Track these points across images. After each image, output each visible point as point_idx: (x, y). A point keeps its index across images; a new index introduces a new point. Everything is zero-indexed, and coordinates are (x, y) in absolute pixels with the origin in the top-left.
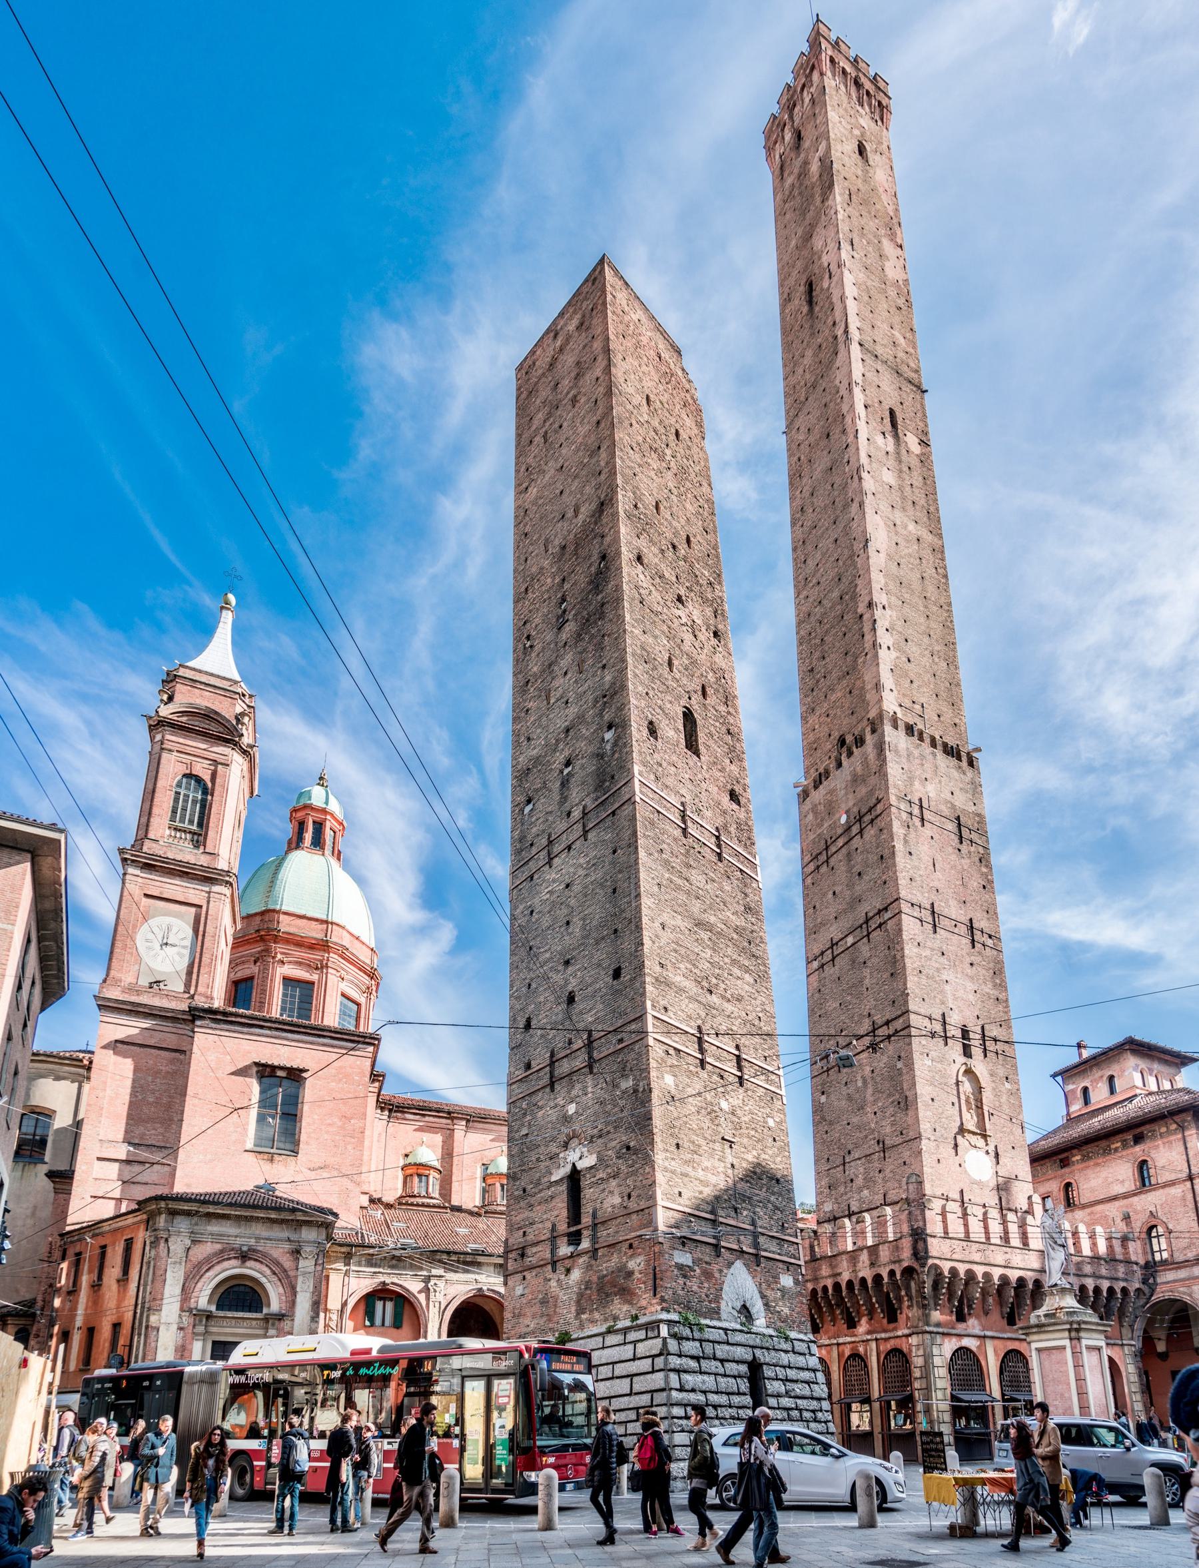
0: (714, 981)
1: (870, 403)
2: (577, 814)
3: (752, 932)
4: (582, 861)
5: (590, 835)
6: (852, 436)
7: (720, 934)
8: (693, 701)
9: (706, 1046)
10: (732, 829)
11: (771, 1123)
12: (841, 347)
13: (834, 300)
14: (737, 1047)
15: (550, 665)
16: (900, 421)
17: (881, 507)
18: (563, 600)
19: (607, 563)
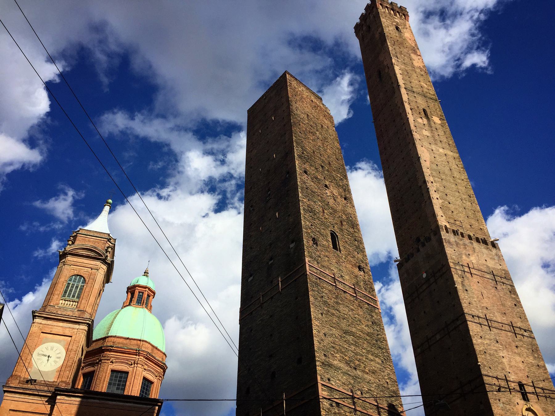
0: (357, 362)
1: (412, 108)
7: (359, 337)
9: (356, 400)
10: (362, 284)
16: (429, 113)
17: (424, 144)
18: (269, 190)
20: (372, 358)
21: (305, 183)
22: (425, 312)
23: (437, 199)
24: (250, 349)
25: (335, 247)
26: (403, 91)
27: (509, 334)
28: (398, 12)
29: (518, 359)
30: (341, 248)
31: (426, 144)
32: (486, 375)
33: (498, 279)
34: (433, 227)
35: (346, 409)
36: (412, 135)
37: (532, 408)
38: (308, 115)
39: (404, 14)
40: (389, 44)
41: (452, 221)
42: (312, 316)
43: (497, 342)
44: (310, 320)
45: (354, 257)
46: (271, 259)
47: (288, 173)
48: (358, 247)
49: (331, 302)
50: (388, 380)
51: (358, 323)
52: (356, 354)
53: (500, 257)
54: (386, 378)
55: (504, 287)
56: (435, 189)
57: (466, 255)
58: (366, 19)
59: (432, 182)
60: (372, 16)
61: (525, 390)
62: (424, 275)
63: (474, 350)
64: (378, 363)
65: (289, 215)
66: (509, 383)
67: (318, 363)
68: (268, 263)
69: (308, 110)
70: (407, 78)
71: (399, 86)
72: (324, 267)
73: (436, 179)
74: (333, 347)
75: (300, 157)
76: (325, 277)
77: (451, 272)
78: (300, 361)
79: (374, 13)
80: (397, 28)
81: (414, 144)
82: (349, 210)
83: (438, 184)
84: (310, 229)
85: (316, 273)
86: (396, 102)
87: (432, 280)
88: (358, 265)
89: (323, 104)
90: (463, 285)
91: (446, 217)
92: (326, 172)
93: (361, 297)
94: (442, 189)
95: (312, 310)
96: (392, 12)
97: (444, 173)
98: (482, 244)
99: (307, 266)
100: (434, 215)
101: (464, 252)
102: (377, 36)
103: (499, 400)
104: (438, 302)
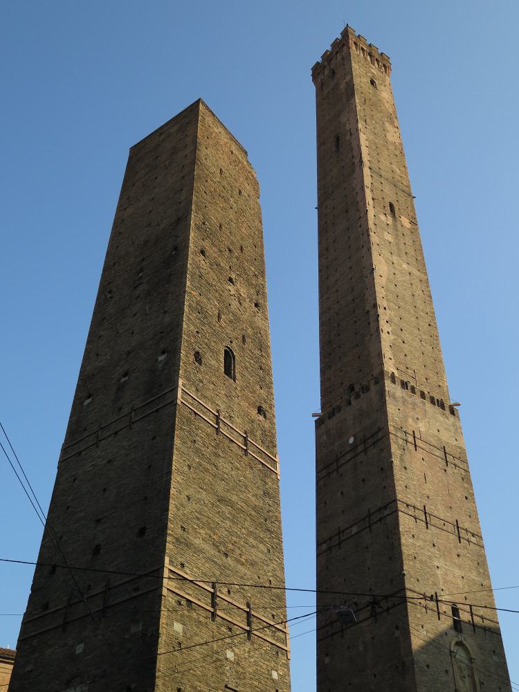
2: (126, 410)
3: (269, 511)
6: (363, 213)
7: (241, 511)
8: (234, 344)
9: (218, 600)
11: (275, 675)
12: (357, 168)
13: (353, 146)
14: (248, 606)
15: (123, 310)
16: (396, 210)
18: (141, 270)
19: (179, 251)
20: (254, 542)
21: (198, 267)
22: (342, 493)
23: (388, 333)
24: (68, 508)
25: (229, 370)
26: (366, 171)
27: (452, 537)
28: (377, 60)
29: (458, 572)
30: (238, 376)
31: (385, 252)
32: (410, 590)
33: (450, 458)
34: (376, 372)
35: (202, 612)
36: (369, 235)
37: (464, 642)
38: (221, 171)
39: (384, 65)
40: (357, 101)
41: (403, 368)
42: (173, 468)
43: (434, 545)
44: (170, 472)
45: (254, 392)
46: (125, 375)
47: (176, 249)
48: (262, 380)
49: (207, 452)
50: (271, 579)
51: (243, 489)
52: (231, 533)
53: (457, 430)
54: (270, 574)
55: (456, 471)
56: (387, 318)
57: (413, 418)
58: (331, 59)
59: (385, 309)
60: (339, 58)
61: (459, 617)
62: (351, 440)
63: (401, 553)
64: (262, 552)
65: (165, 312)
66: (440, 604)
67: (169, 539)
68: (119, 380)
69: (224, 164)
70: (375, 154)
71: (361, 162)
72: (205, 397)
73: (392, 304)
74: (198, 519)
75: (198, 228)
76: (204, 414)
77: (388, 439)
78: (142, 532)
79: (343, 54)
80: (372, 82)
81: (369, 249)
82: (258, 321)
83: (393, 313)
84: (194, 337)
85: (192, 404)
86: (354, 185)
87: (360, 448)
88: (258, 404)
89: (248, 162)
90: (402, 460)
91: (396, 361)
92: (234, 260)
93: (254, 452)
94: (396, 319)
95: (174, 458)
96: (369, 58)
97: (403, 299)
98: (437, 406)
99: (180, 392)
100: (380, 355)
101: (412, 414)
102: (343, 86)
103: (422, 627)
104: (364, 480)
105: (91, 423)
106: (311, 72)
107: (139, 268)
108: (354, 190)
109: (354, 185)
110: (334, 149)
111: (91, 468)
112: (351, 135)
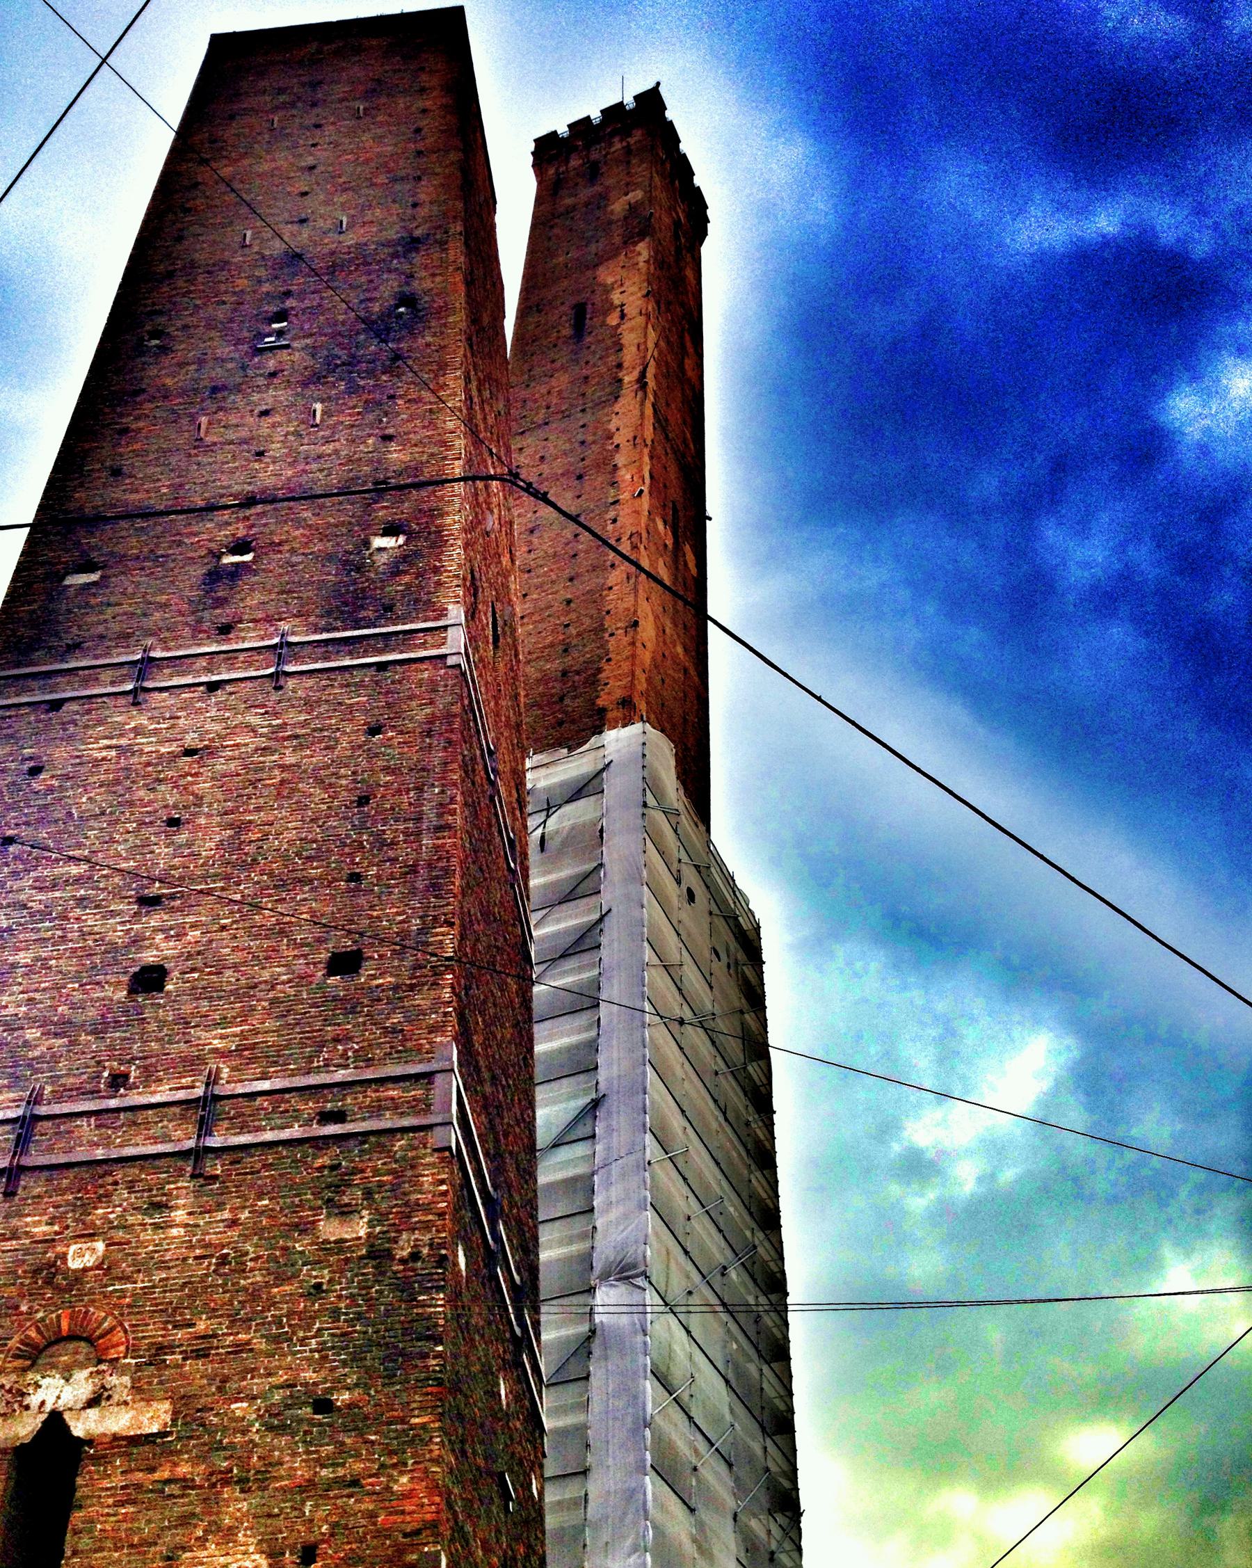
4: (254, 720)
5: (291, 683)
46: (240, 547)
60: (618, 146)
65: (387, 438)
68: (219, 556)
78: (344, 964)
79: (632, 141)
105: (102, 637)
106: (532, 147)
107: (273, 309)
108: (610, 437)
109: (612, 427)
110: (567, 331)
111: (113, 753)
112: (623, 316)
